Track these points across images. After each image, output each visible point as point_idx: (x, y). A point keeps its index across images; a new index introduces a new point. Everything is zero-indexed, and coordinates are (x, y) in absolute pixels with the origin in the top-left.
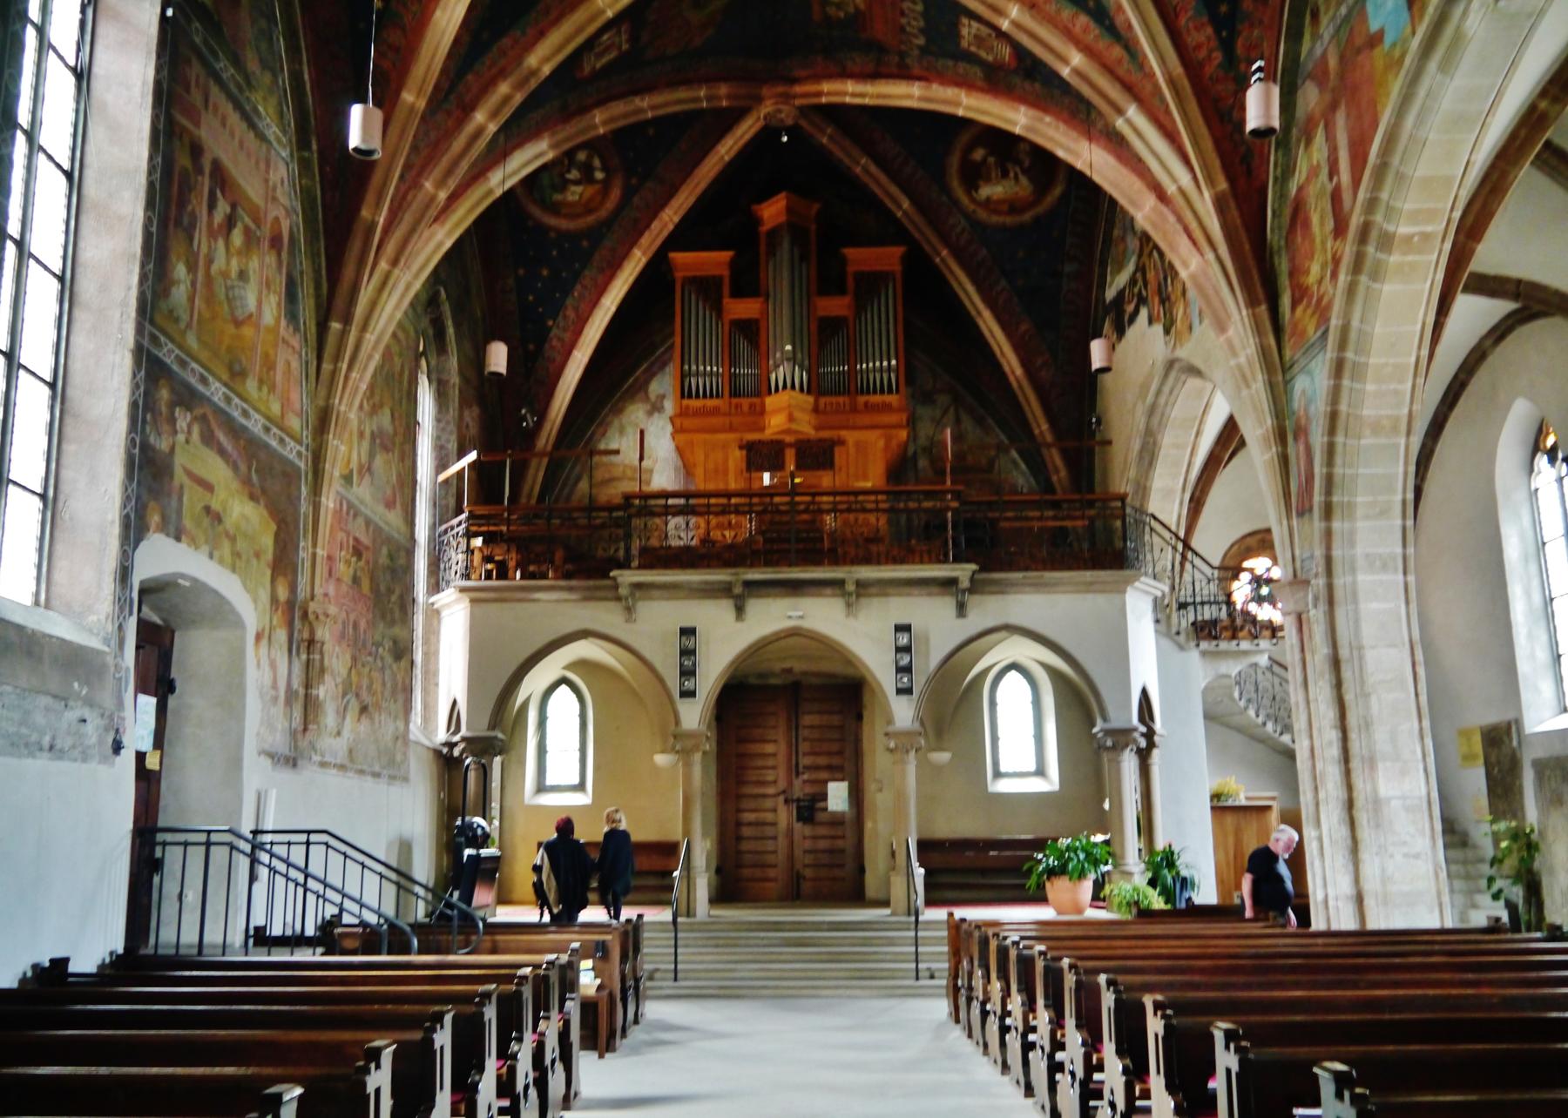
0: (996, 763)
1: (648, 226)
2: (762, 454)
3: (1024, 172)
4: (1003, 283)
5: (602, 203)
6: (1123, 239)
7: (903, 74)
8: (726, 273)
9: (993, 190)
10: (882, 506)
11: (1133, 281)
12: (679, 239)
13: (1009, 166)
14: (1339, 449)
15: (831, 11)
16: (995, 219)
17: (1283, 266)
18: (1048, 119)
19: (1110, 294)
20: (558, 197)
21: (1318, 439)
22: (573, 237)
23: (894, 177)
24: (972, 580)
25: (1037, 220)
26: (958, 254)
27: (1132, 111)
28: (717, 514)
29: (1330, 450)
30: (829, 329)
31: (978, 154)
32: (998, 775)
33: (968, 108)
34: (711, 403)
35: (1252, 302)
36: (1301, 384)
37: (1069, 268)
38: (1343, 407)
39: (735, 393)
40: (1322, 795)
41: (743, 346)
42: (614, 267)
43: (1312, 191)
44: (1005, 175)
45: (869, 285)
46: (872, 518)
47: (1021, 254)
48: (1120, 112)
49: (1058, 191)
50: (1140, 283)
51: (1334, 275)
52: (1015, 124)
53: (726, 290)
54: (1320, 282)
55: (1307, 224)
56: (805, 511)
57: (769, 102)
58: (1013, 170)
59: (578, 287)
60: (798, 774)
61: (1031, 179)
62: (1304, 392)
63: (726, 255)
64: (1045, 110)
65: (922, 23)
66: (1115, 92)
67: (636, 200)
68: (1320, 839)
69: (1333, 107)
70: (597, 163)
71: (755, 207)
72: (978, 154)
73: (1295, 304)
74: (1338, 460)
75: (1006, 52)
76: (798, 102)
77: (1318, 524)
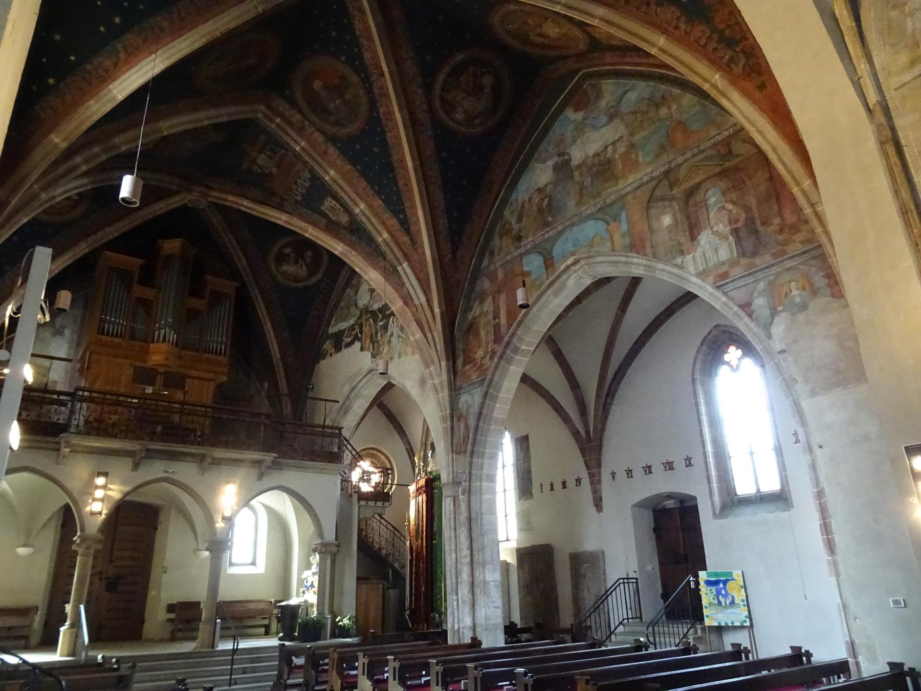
0: (230, 558)
1: (95, 232)
2: (145, 375)
3: (306, 265)
6: (348, 308)
7: (279, 208)
8: (137, 270)
9: (288, 268)
10: (210, 414)
11: (352, 328)
13: (300, 260)
14: (480, 428)
15: (255, 168)
17: (460, 346)
19: (332, 330)
21: (472, 423)
24: (273, 462)
27: (405, 265)
28: (109, 405)
29: (477, 428)
30: (192, 314)
31: (288, 251)
32: (231, 564)
33: (311, 234)
34: (117, 340)
35: (448, 360)
36: (464, 398)
38: (484, 412)
39: (132, 337)
40: (459, 580)
41: (141, 311)
43: (483, 320)
44: (296, 263)
45: (217, 298)
46: (202, 420)
48: (401, 265)
49: (319, 276)
50: (357, 330)
51: (492, 358)
54: (482, 359)
55: (477, 334)
56: (164, 411)
57: (195, 194)
58: (301, 262)
60: (111, 562)
61: (308, 270)
62: (466, 401)
63: (139, 261)
64: (354, 249)
65: (304, 192)
66: (399, 255)
68: (458, 600)
69: (499, 292)
72: (288, 251)
73: (464, 364)
74: (479, 432)
75: (344, 219)
76: (210, 199)
77: (468, 459)
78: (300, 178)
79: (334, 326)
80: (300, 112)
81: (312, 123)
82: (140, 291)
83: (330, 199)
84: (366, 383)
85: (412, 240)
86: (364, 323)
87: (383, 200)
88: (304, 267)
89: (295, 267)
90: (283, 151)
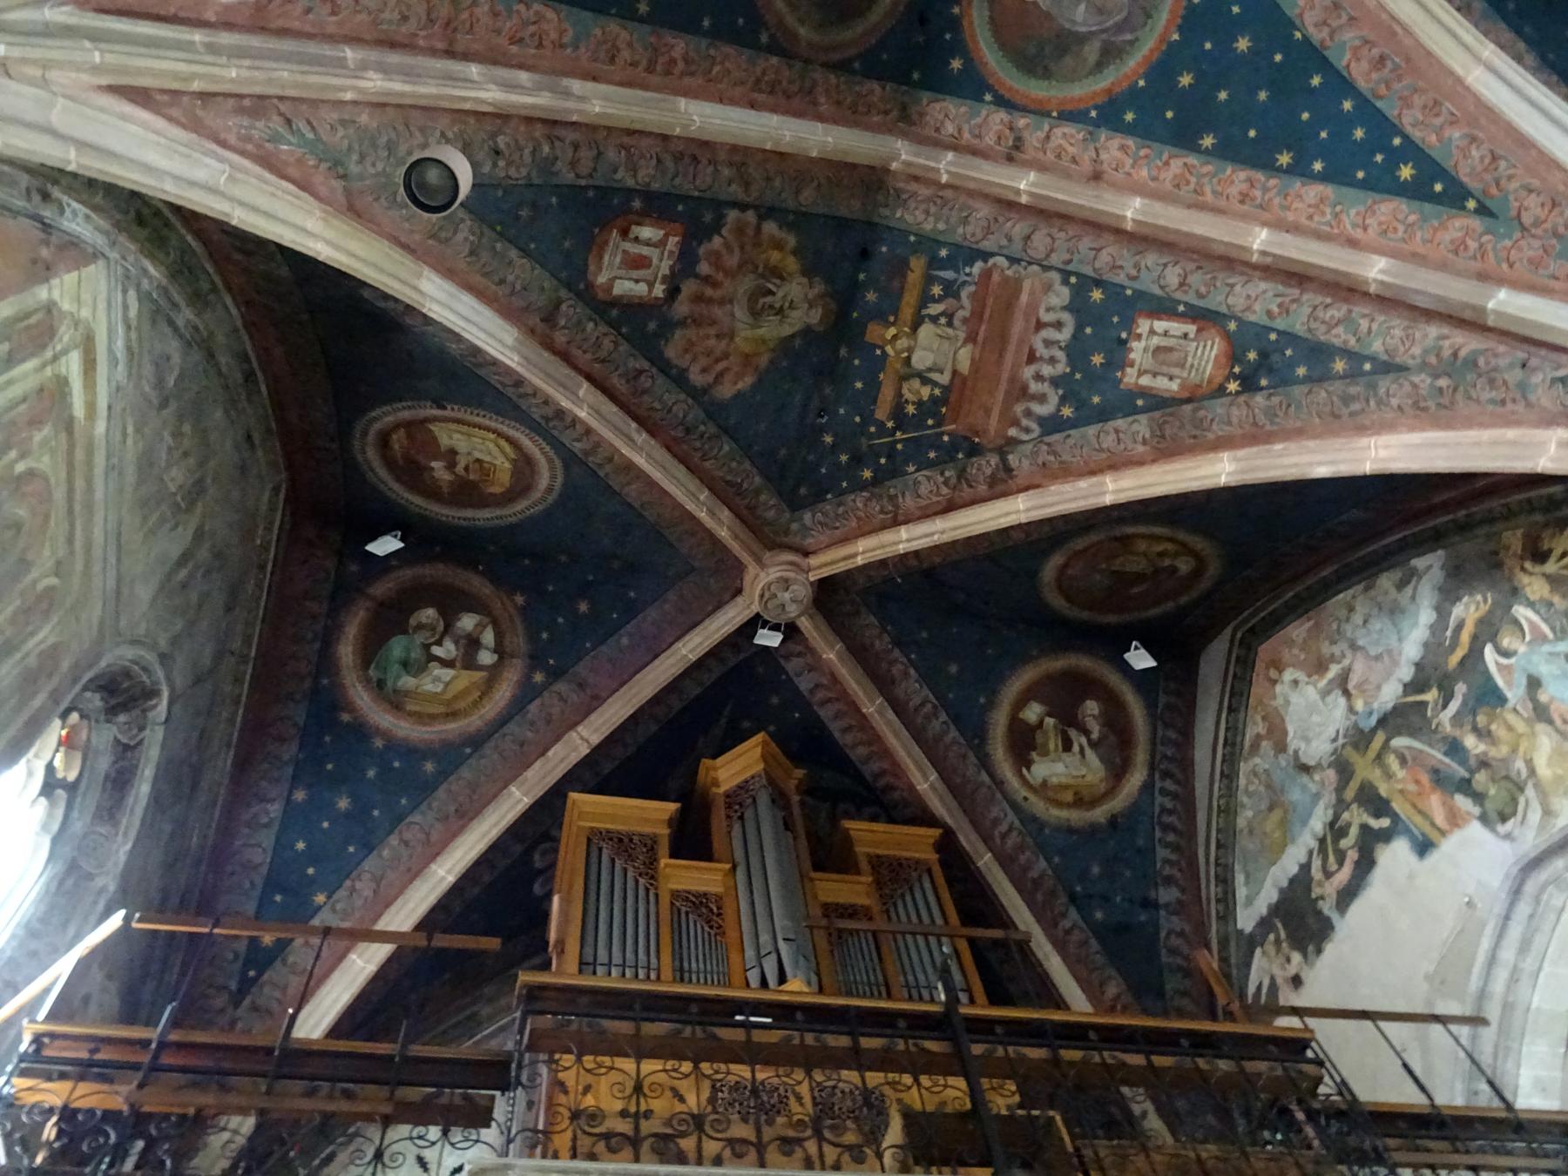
3: (1093, 745)
4: (1073, 914)
5: (476, 704)
7: (1002, 485)
8: (664, 831)
9: (1051, 768)
12: (597, 773)
13: (1073, 733)
16: (1057, 814)
18: (1278, 447)
20: (407, 682)
22: (412, 752)
23: (918, 736)
25: (1113, 821)
26: (1005, 861)
31: (1033, 712)
37: (1167, 895)
41: (696, 928)
42: (466, 816)
45: (892, 875)
47: (1096, 870)
49: (1136, 779)
52: (1219, 475)
53: (664, 848)
58: (1079, 740)
59: (394, 840)
65: (1062, 368)
67: (533, 708)
70: (488, 637)
71: (706, 762)
72: (1033, 712)
75: (1206, 356)
78: (1040, 325)
79: (1250, 901)
80: (1002, 102)
81: (1040, 111)
82: (686, 876)
83: (1143, 325)
84: (1524, 947)
85: (1483, 211)
86: (1375, 776)
87: (1323, 178)
88: (1088, 752)
89: (1072, 759)
90: (978, 267)
